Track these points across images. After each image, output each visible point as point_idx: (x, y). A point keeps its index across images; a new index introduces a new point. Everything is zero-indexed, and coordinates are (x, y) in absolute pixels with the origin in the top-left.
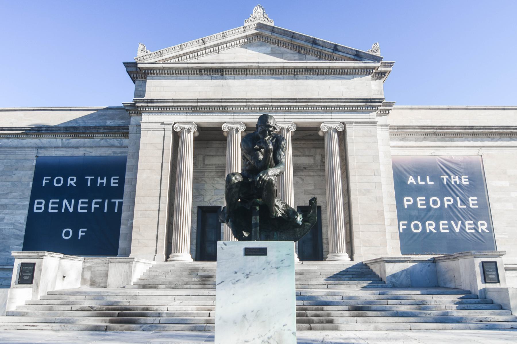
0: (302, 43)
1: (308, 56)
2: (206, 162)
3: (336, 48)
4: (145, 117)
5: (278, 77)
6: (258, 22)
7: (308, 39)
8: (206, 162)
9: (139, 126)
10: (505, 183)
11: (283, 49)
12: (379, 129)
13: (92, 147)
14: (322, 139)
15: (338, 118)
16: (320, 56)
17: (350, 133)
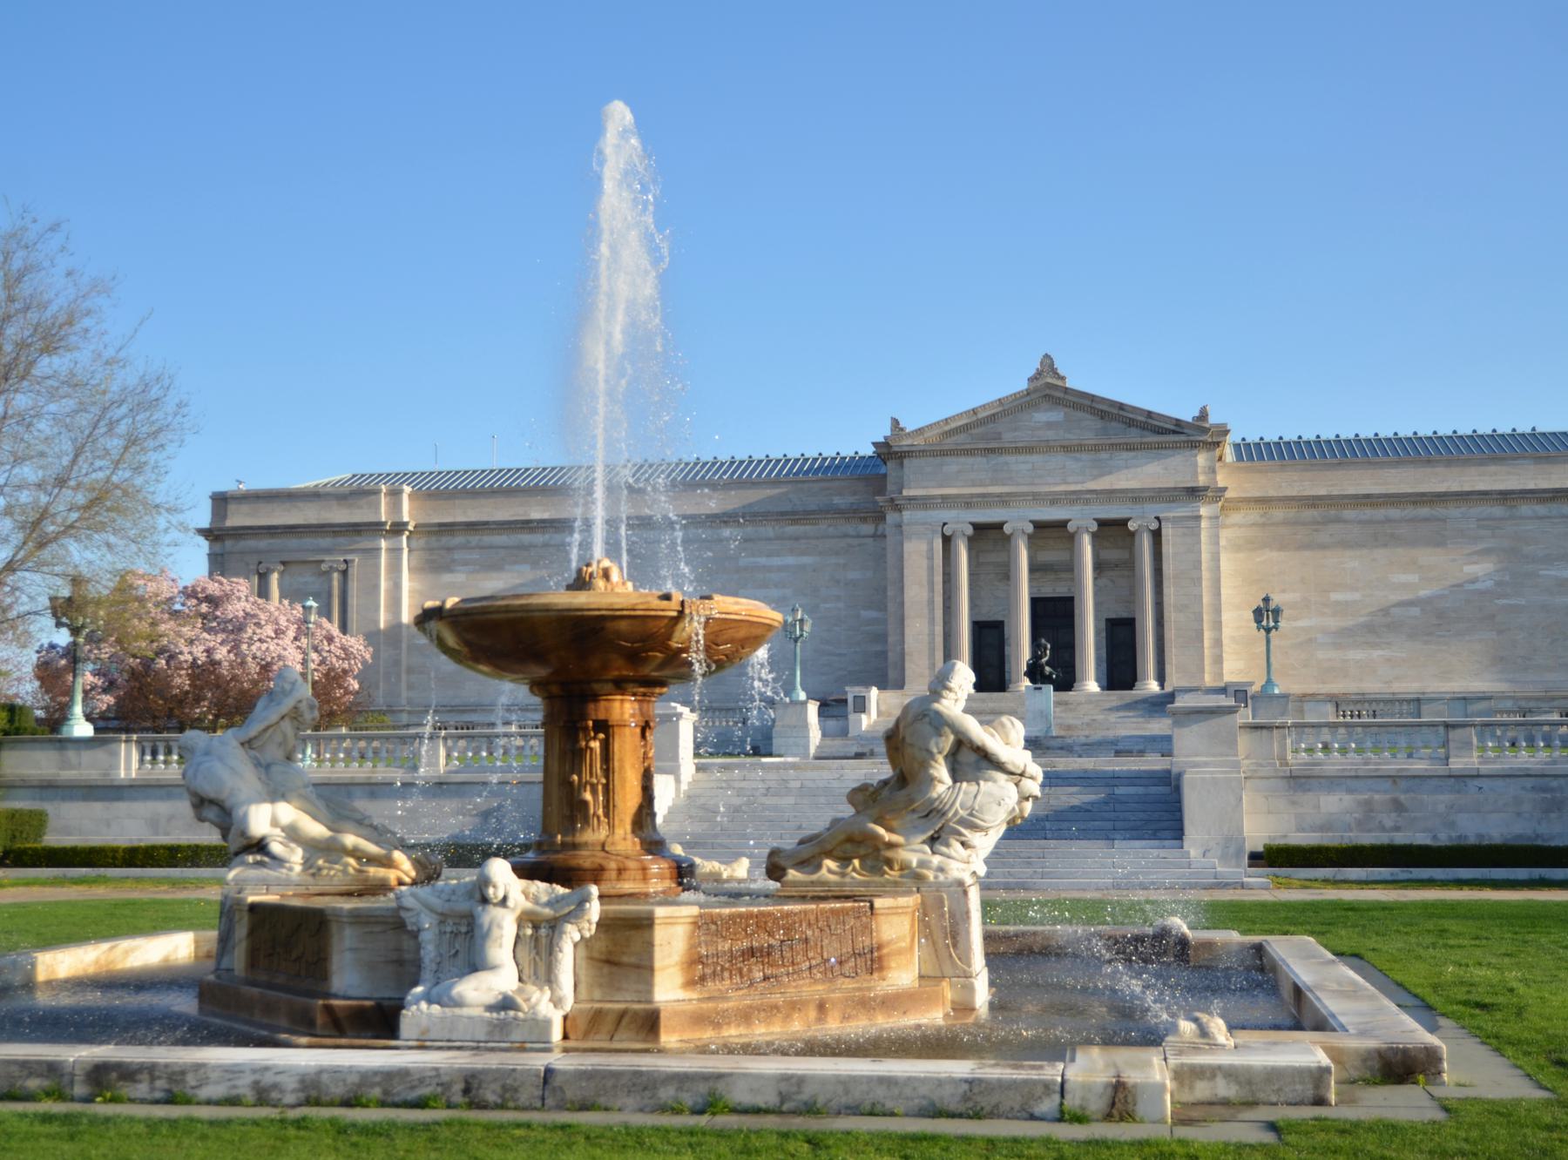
0: (1105, 408)
1: (1114, 424)
2: (981, 560)
3: (1150, 414)
4: (907, 515)
5: (1074, 455)
6: (1043, 382)
7: (1113, 403)
8: (981, 560)
9: (899, 526)
10: (1413, 578)
11: (1080, 414)
12: (1204, 524)
13: (817, 538)
14: (1132, 534)
15: (1152, 510)
16: (1131, 423)
17: (1168, 532)
